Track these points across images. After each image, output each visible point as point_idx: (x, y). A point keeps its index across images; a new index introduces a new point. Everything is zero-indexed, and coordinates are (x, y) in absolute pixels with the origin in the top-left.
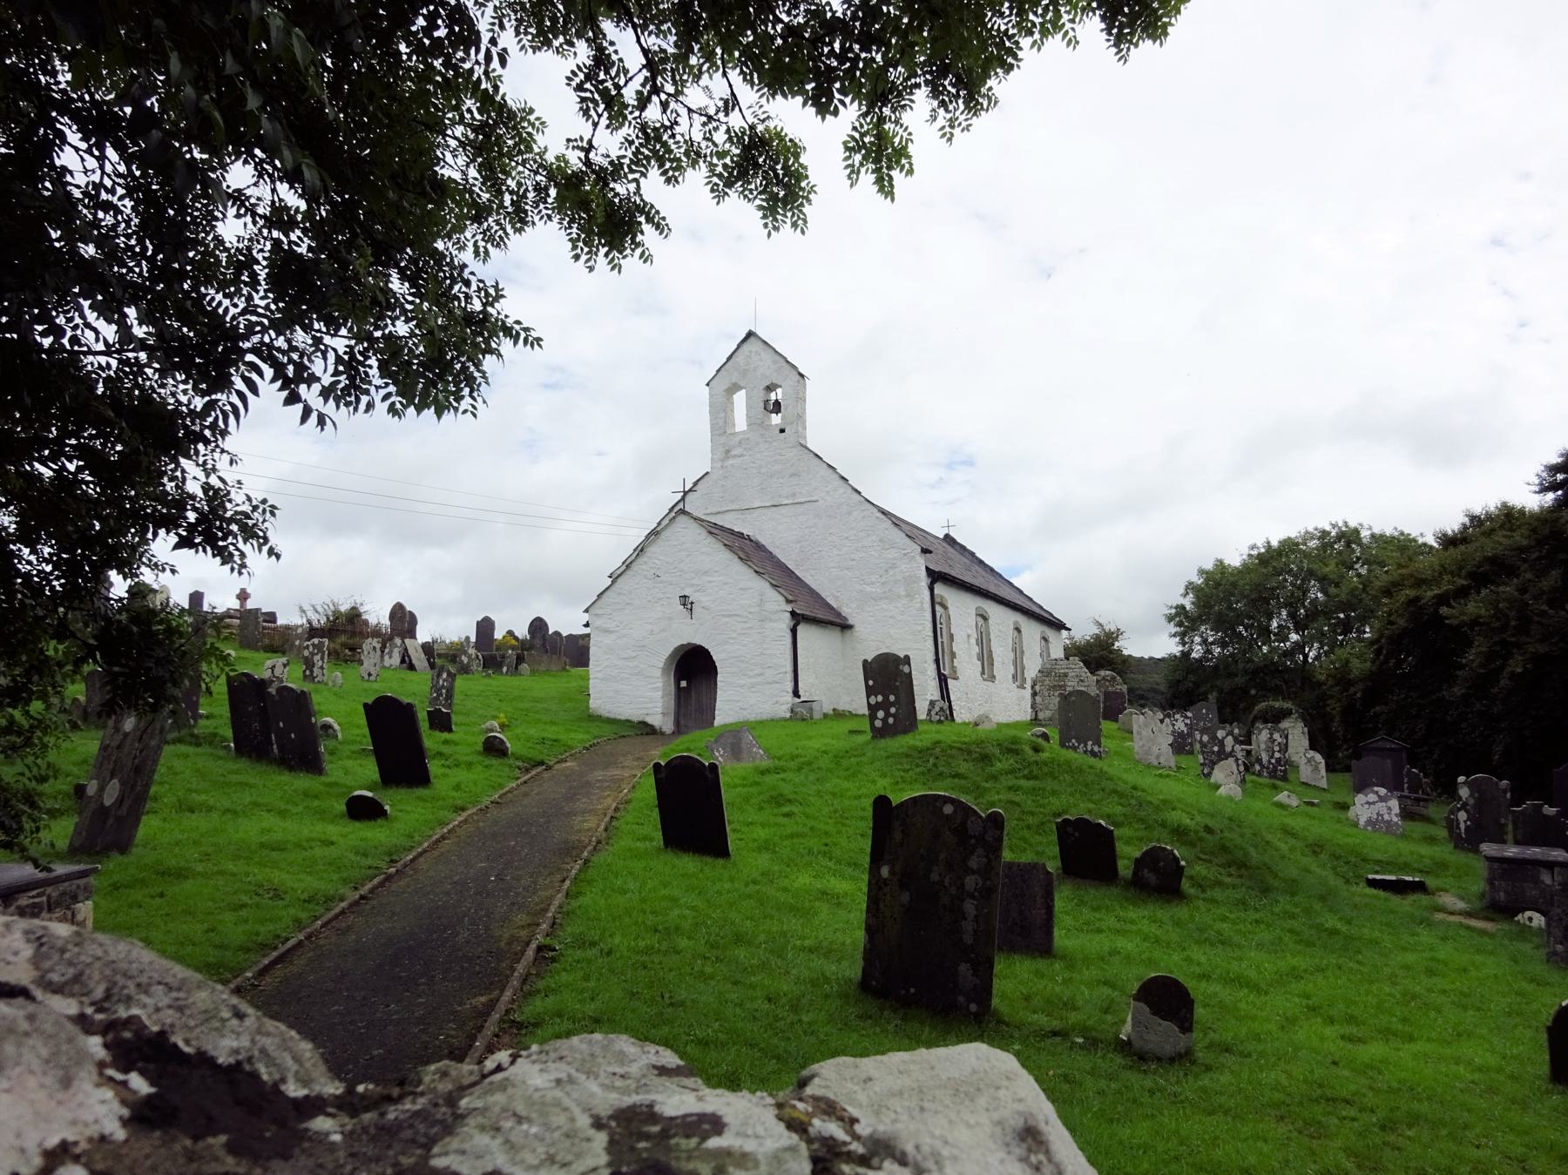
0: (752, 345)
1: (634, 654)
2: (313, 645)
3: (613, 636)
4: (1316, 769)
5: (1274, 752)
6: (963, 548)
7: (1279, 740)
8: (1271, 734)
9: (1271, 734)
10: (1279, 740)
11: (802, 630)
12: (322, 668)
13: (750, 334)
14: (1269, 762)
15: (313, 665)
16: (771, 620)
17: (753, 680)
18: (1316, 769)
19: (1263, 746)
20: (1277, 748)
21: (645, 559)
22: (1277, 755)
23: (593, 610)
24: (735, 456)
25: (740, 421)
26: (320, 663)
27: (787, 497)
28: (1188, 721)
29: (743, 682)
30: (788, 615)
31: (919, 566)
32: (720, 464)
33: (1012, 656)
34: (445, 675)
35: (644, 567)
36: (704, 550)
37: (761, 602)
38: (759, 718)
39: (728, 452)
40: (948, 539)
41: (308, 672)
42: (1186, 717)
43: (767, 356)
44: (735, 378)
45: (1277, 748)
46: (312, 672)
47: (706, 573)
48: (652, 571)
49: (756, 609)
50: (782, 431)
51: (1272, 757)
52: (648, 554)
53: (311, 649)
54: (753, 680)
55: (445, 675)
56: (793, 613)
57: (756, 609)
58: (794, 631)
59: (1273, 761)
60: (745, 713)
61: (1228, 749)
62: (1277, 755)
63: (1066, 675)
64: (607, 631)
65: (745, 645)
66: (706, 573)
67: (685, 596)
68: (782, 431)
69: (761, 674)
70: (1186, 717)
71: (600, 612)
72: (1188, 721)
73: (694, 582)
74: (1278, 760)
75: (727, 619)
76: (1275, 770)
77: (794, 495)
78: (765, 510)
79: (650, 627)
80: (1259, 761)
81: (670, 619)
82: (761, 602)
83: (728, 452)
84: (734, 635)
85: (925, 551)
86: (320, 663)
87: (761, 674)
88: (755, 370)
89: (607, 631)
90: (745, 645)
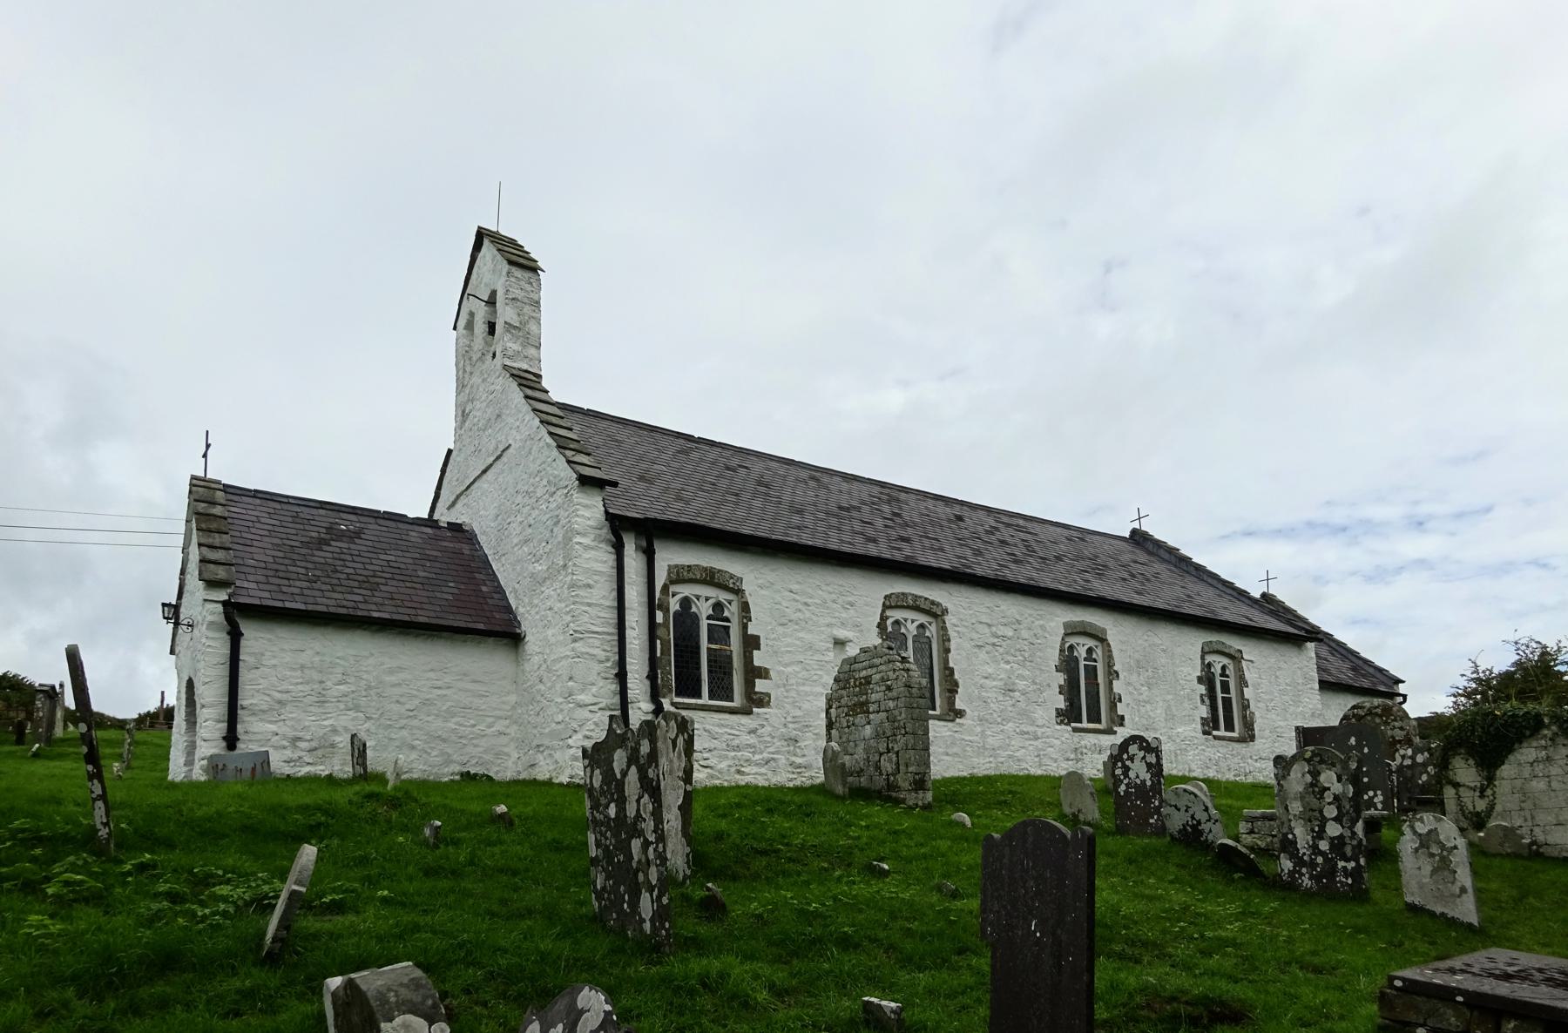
4: (1443, 866)
5: (1323, 821)
6: (1159, 544)
7: (1337, 788)
8: (1315, 774)
9: (1315, 774)
10: (1337, 788)
11: (256, 638)
14: (1315, 850)
18: (1443, 866)
19: (1296, 807)
20: (1330, 812)
22: (1333, 830)
23: (177, 650)
30: (220, 608)
31: (590, 510)
33: (1061, 678)
40: (1139, 538)
45: (1330, 812)
51: (1320, 834)
56: (225, 603)
58: (235, 637)
59: (1324, 846)
61: (631, 811)
62: (1333, 830)
63: (868, 680)
74: (1338, 844)
76: (1331, 871)
80: (1289, 846)
85: (585, 482)
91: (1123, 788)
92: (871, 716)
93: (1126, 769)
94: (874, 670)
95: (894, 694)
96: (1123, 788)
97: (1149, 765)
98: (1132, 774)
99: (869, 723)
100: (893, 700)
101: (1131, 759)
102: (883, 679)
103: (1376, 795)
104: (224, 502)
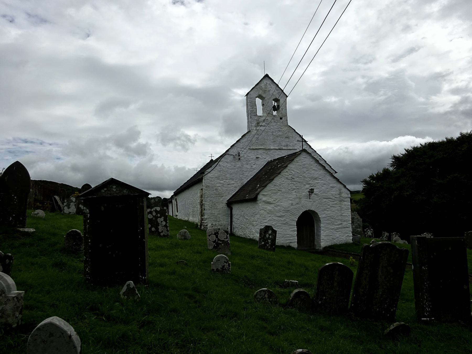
0: (267, 81)
1: (283, 214)
2: (156, 211)
3: (273, 206)
12: (166, 226)
13: (267, 76)
15: (158, 224)
16: (344, 201)
17: (338, 226)
21: (287, 170)
24: (261, 126)
25: (260, 112)
26: (164, 223)
27: (284, 146)
28: (372, 232)
29: (333, 227)
32: (255, 128)
34: (270, 232)
35: (286, 174)
36: (314, 168)
37: (340, 193)
38: (341, 243)
39: (258, 123)
41: (153, 229)
42: (371, 231)
43: (274, 87)
44: (261, 92)
46: (157, 229)
47: (316, 179)
48: (290, 176)
49: (338, 196)
50: (281, 119)
52: (288, 168)
53: (154, 214)
54: (338, 226)
55: (270, 232)
57: (338, 196)
60: (335, 241)
64: (269, 203)
65: (333, 211)
66: (316, 179)
67: (312, 189)
68: (281, 119)
69: (341, 224)
70: (371, 231)
71: (265, 193)
72: (372, 232)
73: (309, 182)
75: (326, 200)
77: (287, 146)
78: (275, 151)
79: (291, 202)
81: (300, 198)
82: (340, 193)
83: (258, 123)
84: (329, 207)
86: (164, 223)
87: (341, 224)
88: (269, 91)
89: (269, 203)
90: (333, 211)
91: (367, 236)
92: (355, 224)
93: (367, 233)
94: (355, 216)
95: (360, 221)
96: (367, 236)
97: (371, 233)
98: (368, 234)
99: (354, 225)
100: (359, 222)
101: (368, 232)
102: (357, 218)
103: (160, 217)
104: (271, 146)
